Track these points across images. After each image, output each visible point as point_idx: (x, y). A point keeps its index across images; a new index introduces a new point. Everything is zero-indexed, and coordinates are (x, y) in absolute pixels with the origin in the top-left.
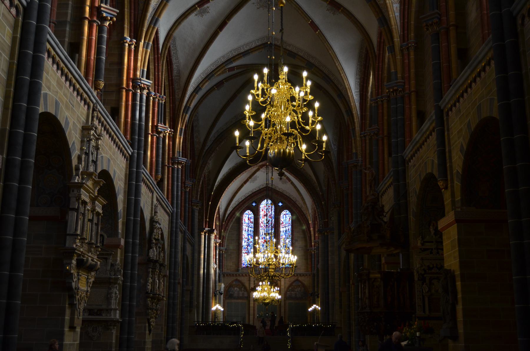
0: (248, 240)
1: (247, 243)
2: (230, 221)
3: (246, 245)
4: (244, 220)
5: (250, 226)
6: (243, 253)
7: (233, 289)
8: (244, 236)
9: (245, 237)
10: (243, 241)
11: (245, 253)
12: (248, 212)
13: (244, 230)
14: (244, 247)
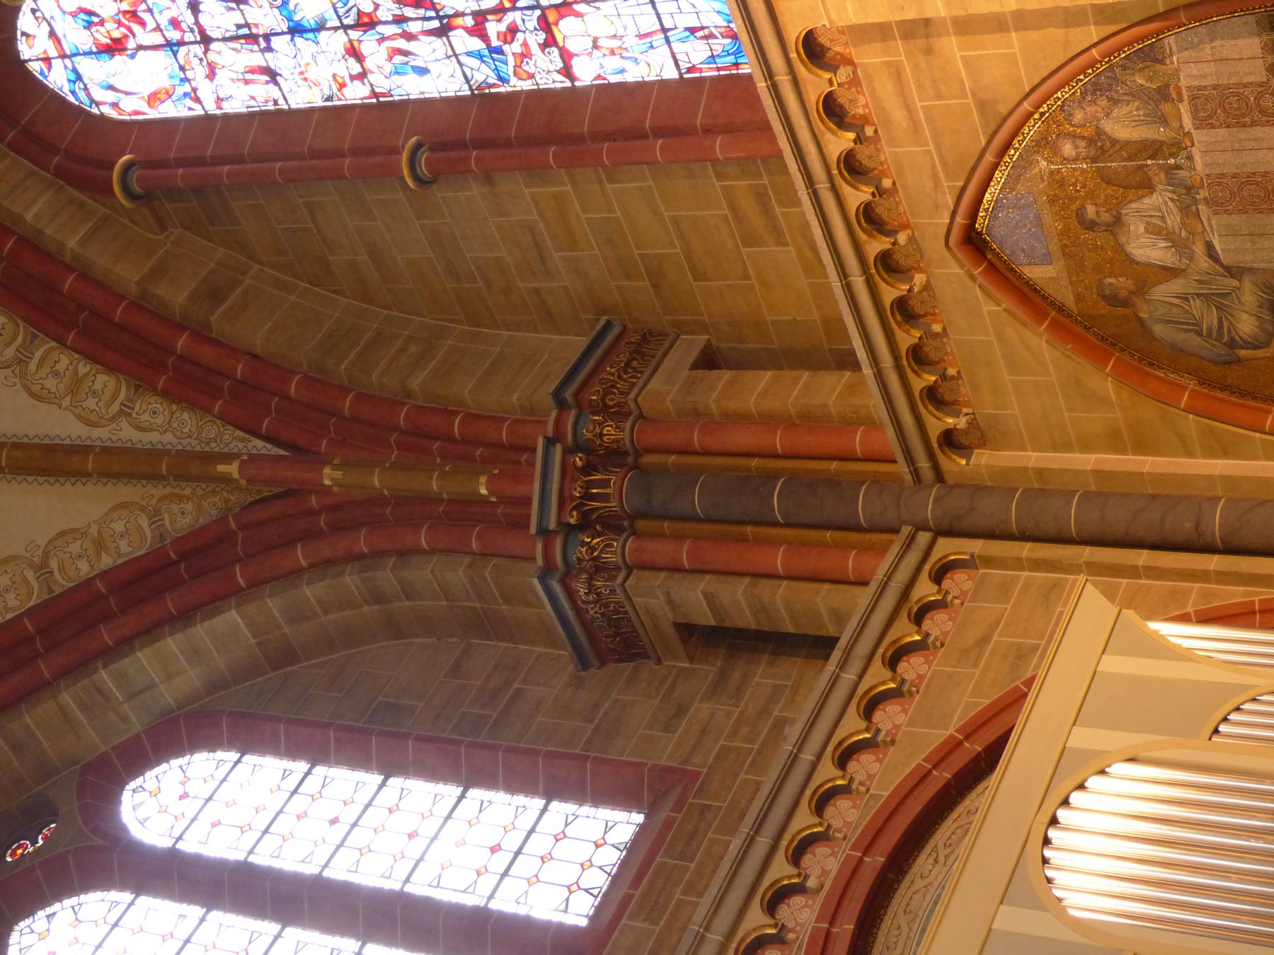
0: (366, 22)
1: (409, 37)
2: (208, 354)
3: (438, 43)
4: (153, 99)
5: (188, 18)
6: (567, 71)
7: (1164, 292)
8: (343, 85)
9: (344, 74)
10: (411, 87)
11: (550, 42)
12: (47, 60)
13: (273, 91)
14: (483, 74)
